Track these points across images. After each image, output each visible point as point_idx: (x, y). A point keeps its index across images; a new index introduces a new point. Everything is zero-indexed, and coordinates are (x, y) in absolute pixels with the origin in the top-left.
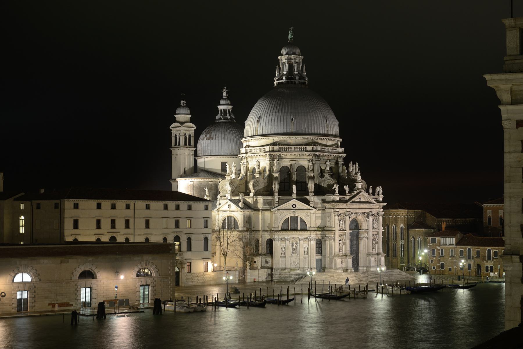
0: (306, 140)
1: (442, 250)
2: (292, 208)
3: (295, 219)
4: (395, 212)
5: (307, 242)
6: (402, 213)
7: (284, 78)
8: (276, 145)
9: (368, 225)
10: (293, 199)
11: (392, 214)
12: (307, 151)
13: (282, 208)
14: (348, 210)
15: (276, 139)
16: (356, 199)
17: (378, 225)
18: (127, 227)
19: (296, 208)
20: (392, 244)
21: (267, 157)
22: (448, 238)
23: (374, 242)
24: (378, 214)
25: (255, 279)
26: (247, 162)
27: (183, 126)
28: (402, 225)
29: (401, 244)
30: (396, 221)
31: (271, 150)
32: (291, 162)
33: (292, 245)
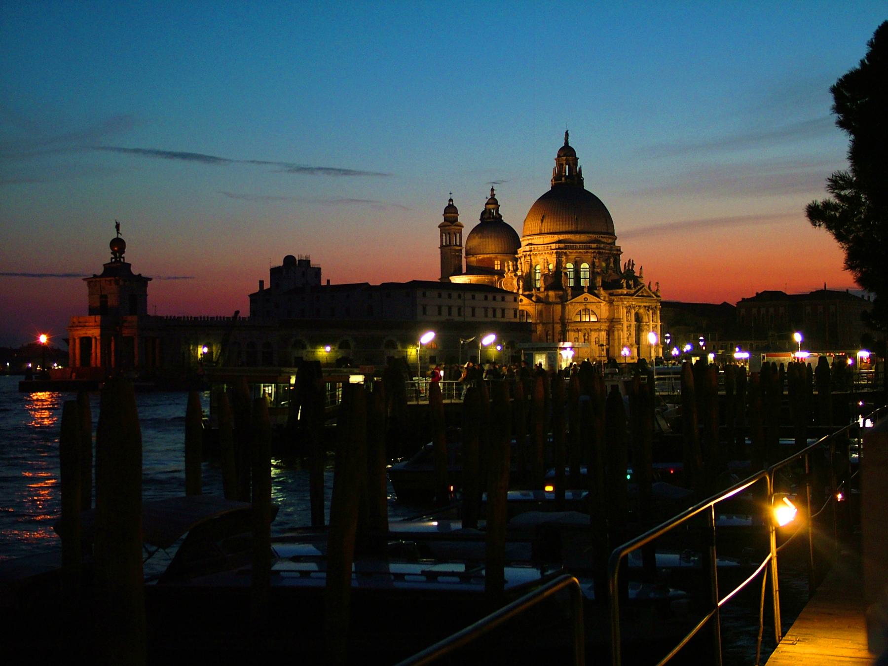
2: (583, 301)
5: (598, 333)
7: (563, 179)
8: (562, 243)
9: (648, 318)
10: (585, 292)
12: (591, 248)
13: (575, 301)
14: (634, 303)
15: (562, 237)
16: (639, 293)
18: (459, 314)
19: (588, 301)
21: (553, 254)
24: (656, 307)
26: (531, 259)
27: (454, 224)
31: (557, 247)
32: (576, 259)
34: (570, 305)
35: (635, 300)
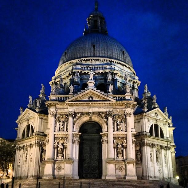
3: (28, 126)
9: (108, 127)
14: (71, 110)
17: (126, 127)
23: (120, 146)
33: (25, 153)
35: (74, 107)
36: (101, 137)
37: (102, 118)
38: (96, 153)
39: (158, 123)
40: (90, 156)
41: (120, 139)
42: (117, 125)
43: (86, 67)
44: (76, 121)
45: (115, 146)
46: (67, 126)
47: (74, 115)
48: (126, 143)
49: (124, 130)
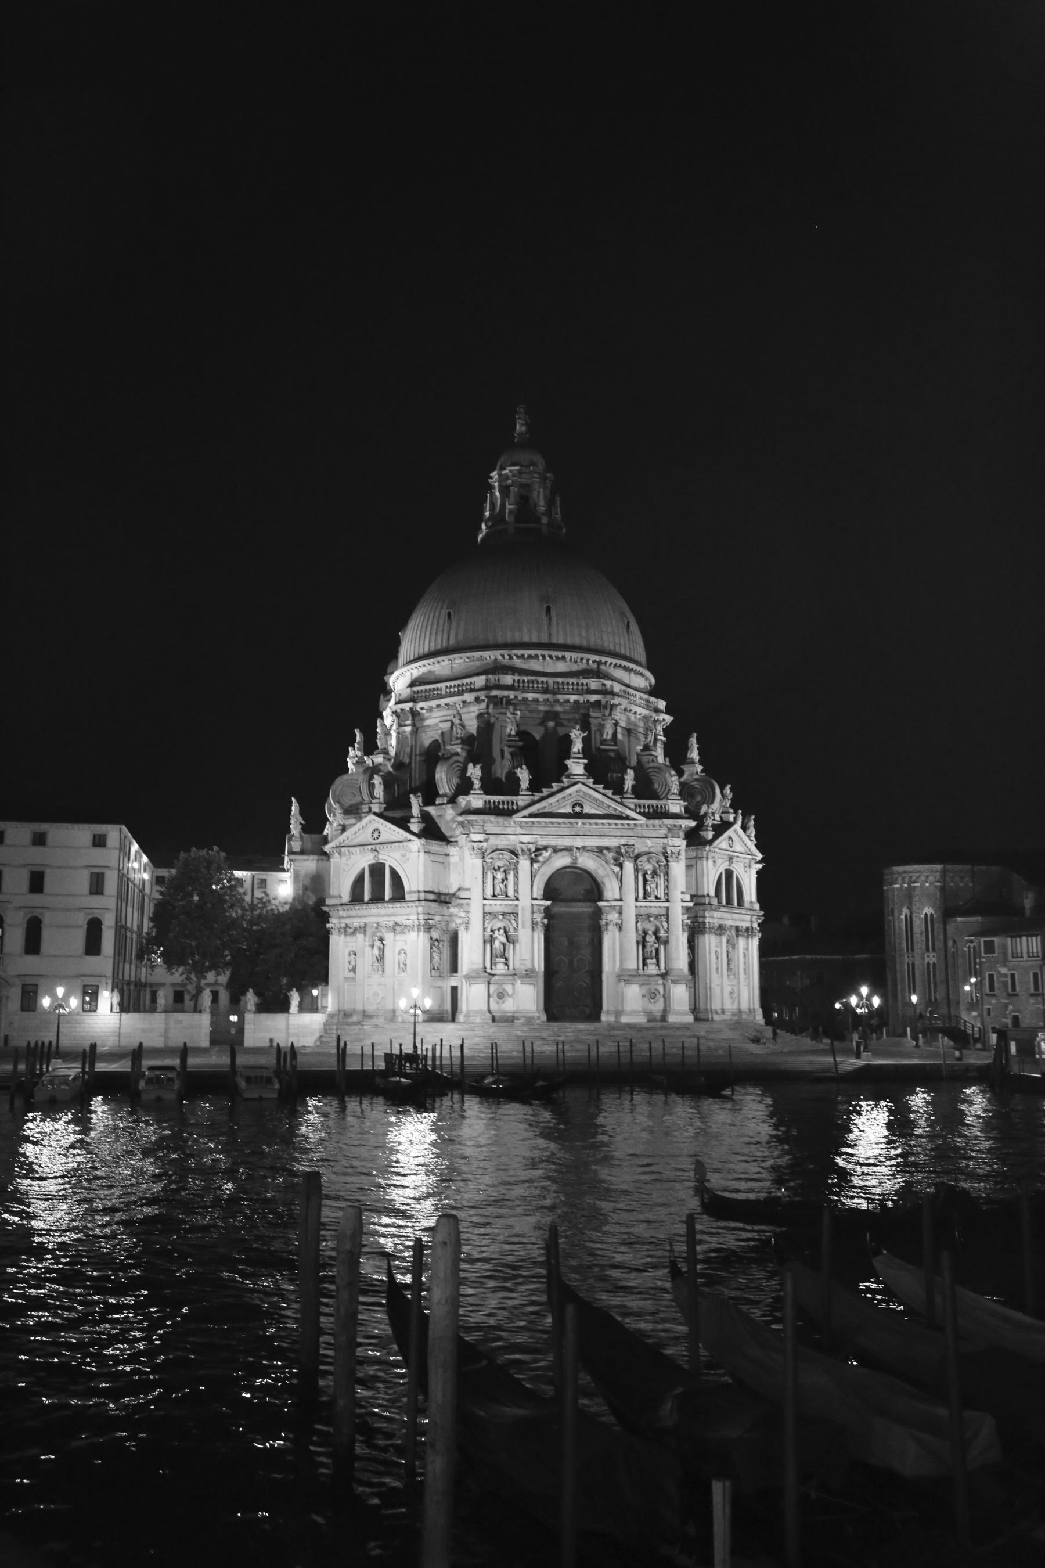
0: (478, 663)
1: (1013, 976)
3: (377, 870)
4: (905, 872)
6: (926, 874)
9: (621, 888)
11: (900, 879)
13: (346, 843)
14: (526, 839)
17: (667, 887)
20: (902, 963)
22: (1024, 939)
23: (651, 939)
25: (271, 1041)
28: (928, 910)
29: (928, 964)
30: (909, 896)
33: (373, 946)
34: (336, 855)
36: (598, 913)
37: (607, 862)
38: (586, 953)
39: (733, 865)
40: (571, 962)
41: (652, 919)
42: (645, 881)
43: (528, 681)
44: (539, 868)
45: (640, 939)
46: (516, 884)
47: (536, 854)
48: (667, 931)
49: (661, 895)
